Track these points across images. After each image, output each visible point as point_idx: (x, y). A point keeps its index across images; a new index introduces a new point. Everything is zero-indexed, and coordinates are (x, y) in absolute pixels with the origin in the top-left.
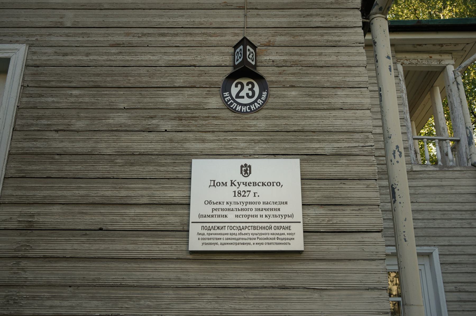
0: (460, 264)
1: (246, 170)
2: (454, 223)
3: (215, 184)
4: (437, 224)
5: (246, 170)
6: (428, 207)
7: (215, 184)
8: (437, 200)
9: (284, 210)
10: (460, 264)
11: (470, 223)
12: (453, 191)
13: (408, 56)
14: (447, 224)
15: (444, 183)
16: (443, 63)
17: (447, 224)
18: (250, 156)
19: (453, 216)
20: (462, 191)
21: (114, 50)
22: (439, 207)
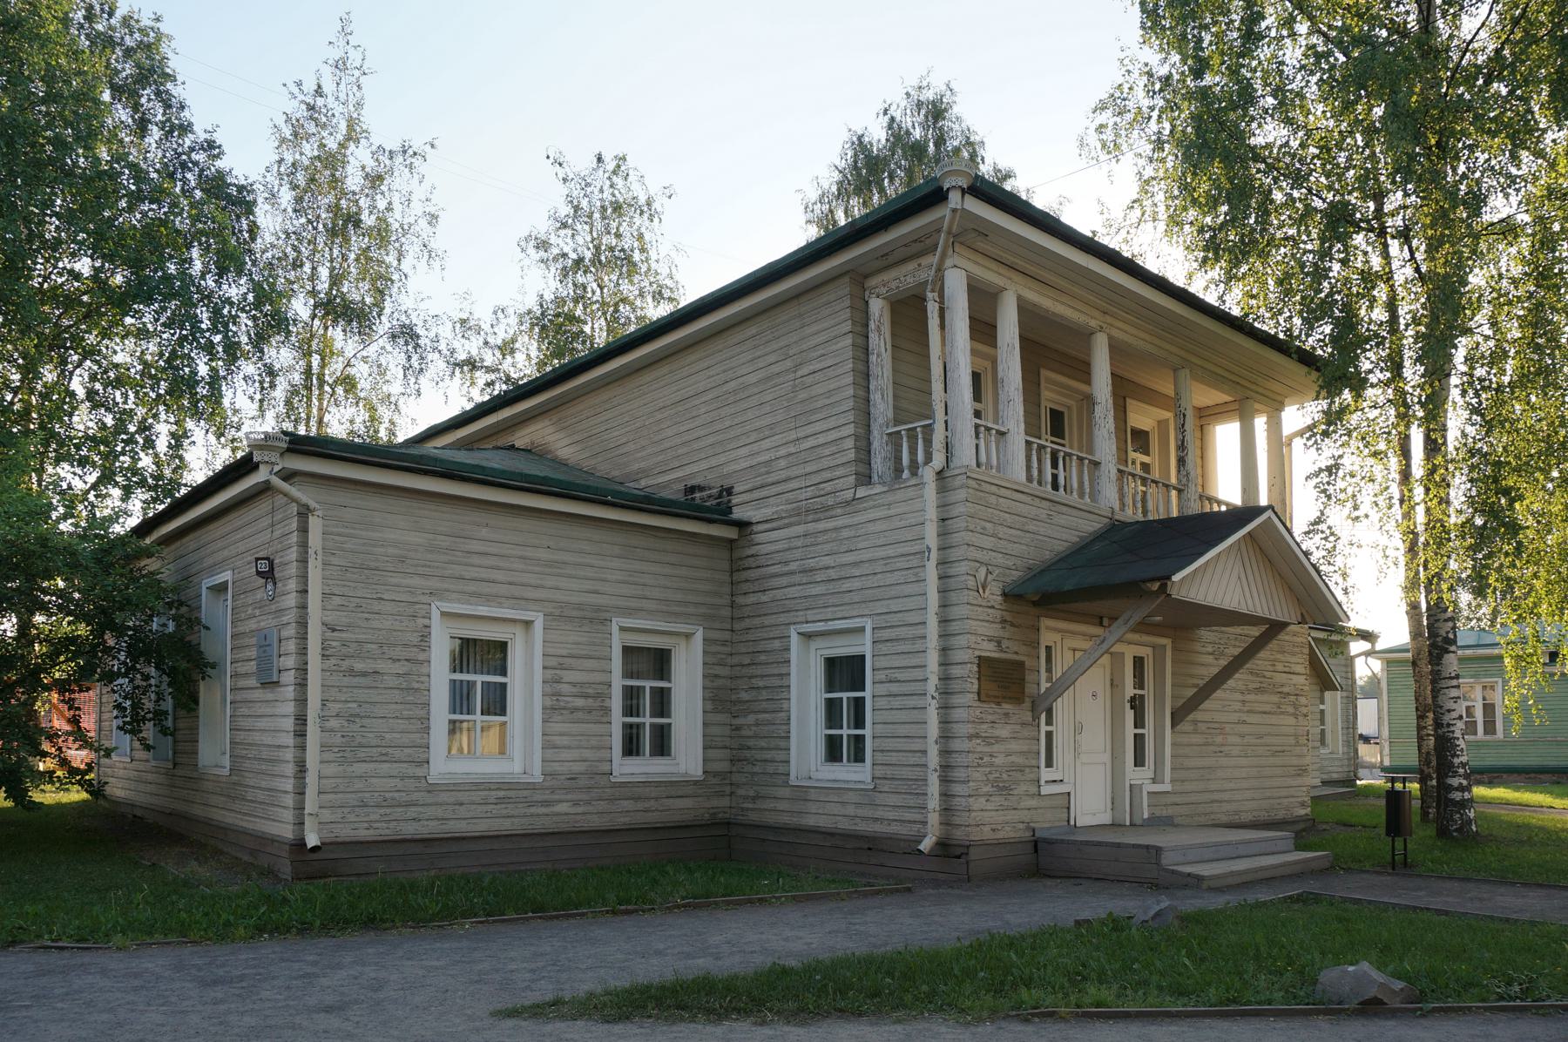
0: (897, 640)
10: (897, 640)
11: (916, 574)
12: (903, 523)
14: (890, 579)
15: (892, 512)
17: (890, 579)
19: (899, 565)
22: (881, 553)
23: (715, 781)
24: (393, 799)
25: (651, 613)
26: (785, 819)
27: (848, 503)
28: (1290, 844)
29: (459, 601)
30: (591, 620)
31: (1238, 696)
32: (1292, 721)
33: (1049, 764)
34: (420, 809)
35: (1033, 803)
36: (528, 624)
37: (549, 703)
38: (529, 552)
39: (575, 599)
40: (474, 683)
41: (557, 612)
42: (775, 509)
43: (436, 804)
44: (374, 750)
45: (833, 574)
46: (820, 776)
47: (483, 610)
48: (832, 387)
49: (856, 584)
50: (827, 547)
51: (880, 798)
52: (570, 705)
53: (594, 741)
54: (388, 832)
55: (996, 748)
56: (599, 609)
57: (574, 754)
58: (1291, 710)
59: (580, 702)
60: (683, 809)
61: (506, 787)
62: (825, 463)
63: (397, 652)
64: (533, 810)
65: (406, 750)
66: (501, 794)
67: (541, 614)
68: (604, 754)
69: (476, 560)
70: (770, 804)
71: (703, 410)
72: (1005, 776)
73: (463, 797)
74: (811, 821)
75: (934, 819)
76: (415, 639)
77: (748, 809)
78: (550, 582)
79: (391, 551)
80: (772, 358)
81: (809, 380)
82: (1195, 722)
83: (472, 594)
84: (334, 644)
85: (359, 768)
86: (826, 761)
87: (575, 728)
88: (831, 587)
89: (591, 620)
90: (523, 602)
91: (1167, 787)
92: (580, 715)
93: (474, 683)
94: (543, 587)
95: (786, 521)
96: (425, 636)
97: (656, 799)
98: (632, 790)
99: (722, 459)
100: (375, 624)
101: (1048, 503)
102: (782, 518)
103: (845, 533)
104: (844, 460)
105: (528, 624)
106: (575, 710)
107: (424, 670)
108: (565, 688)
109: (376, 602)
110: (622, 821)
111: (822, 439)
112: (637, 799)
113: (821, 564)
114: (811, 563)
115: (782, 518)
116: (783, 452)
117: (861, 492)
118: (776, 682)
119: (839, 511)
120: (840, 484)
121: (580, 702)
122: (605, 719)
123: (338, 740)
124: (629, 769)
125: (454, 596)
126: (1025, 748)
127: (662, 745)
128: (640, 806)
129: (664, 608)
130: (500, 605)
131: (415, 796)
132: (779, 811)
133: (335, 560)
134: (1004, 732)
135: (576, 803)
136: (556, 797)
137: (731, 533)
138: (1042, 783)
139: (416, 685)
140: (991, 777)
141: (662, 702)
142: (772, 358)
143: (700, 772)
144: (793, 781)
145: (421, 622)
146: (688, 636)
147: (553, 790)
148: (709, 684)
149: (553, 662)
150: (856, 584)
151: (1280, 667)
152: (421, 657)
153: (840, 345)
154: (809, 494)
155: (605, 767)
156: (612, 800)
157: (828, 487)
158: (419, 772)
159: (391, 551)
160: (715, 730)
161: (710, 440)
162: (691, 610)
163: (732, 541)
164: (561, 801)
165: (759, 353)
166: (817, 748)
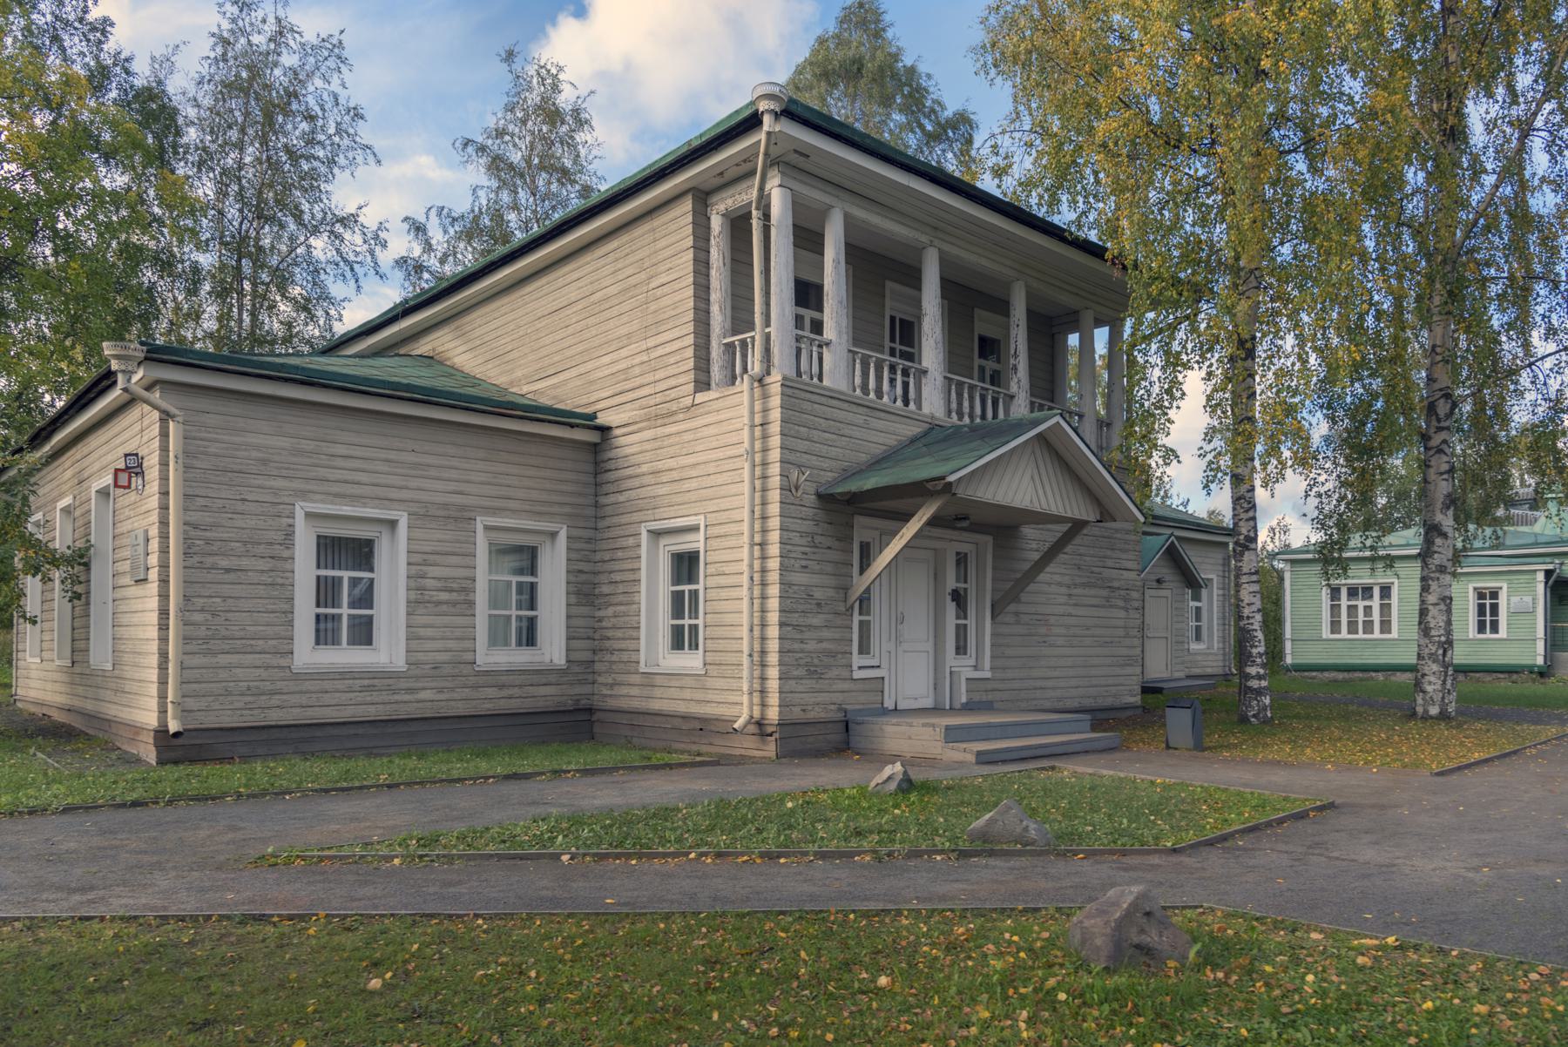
14: (720, 479)
17: (720, 479)
23: (577, 669)
24: (257, 687)
25: (515, 512)
26: (636, 704)
27: (688, 408)
28: (1088, 728)
29: (323, 502)
30: (456, 519)
31: (1064, 590)
32: (1122, 614)
33: (864, 649)
34: (285, 697)
35: (846, 686)
36: (393, 524)
37: (413, 595)
38: (392, 455)
39: (440, 498)
40: (340, 579)
41: (422, 511)
43: (301, 692)
44: (238, 642)
45: (675, 475)
47: (347, 510)
48: (677, 299)
51: (710, 682)
52: (435, 599)
53: (458, 632)
54: (252, 718)
55: (807, 635)
56: (463, 508)
57: (439, 645)
58: (1121, 603)
59: (444, 596)
60: (546, 696)
61: (370, 675)
63: (261, 549)
64: (397, 697)
65: (270, 642)
66: (366, 682)
67: (405, 514)
68: (467, 644)
69: (340, 462)
70: (624, 690)
71: (574, 320)
72: (816, 661)
73: (327, 685)
74: (656, 705)
76: (279, 537)
77: (606, 696)
78: (414, 483)
79: (255, 454)
80: (629, 271)
81: (659, 292)
82: (1017, 614)
83: (336, 495)
84: (198, 542)
85: (224, 659)
86: (673, 648)
87: (439, 620)
89: (456, 519)
90: (386, 502)
91: (988, 675)
92: (444, 608)
93: (340, 579)
94: (407, 488)
96: (289, 534)
97: (520, 686)
98: (493, 677)
99: (589, 366)
100: (239, 523)
101: (865, 410)
103: (687, 437)
104: (685, 368)
105: (393, 524)
106: (439, 603)
107: (288, 566)
108: (429, 583)
109: (240, 503)
110: (486, 707)
111: (668, 348)
112: (502, 687)
113: (666, 466)
114: (660, 465)
116: (637, 360)
117: (700, 397)
118: (630, 576)
121: (444, 596)
122: (469, 612)
123: (202, 632)
124: (489, 657)
125: (318, 497)
126: (837, 636)
127: (529, 636)
128: (506, 692)
129: (528, 508)
130: (365, 505)
131: (279, 685)
132: (629, 697)
133: (197, 464)
134: (816, 621)
135: (440, 690)
136: (420, 685)
137: (592, 437)
138: (855, 667)
139: (280, 581)
140: (802, 662)
141: (530, 596)
142: (629, 271)
143: (563, 662)
144: (643, 668)
145: (286, 521)
146: (553, 535)
147: (417, 678)
148: (573, 579)
149: (417, 558)
150: (693, 484)
151: (1110, 563)
152: (286, 554)
153: (684, 259)
154: (658, 400)
155: (468, 657)
156: (476, 687)
158: (283, 662)
159: (255, 454)
160: (576, 622)
161: (580, 348)
162: (556, 509)
163: (595, 445)
164: (424, 689)
165: (620, 266)
166: (664, 637)
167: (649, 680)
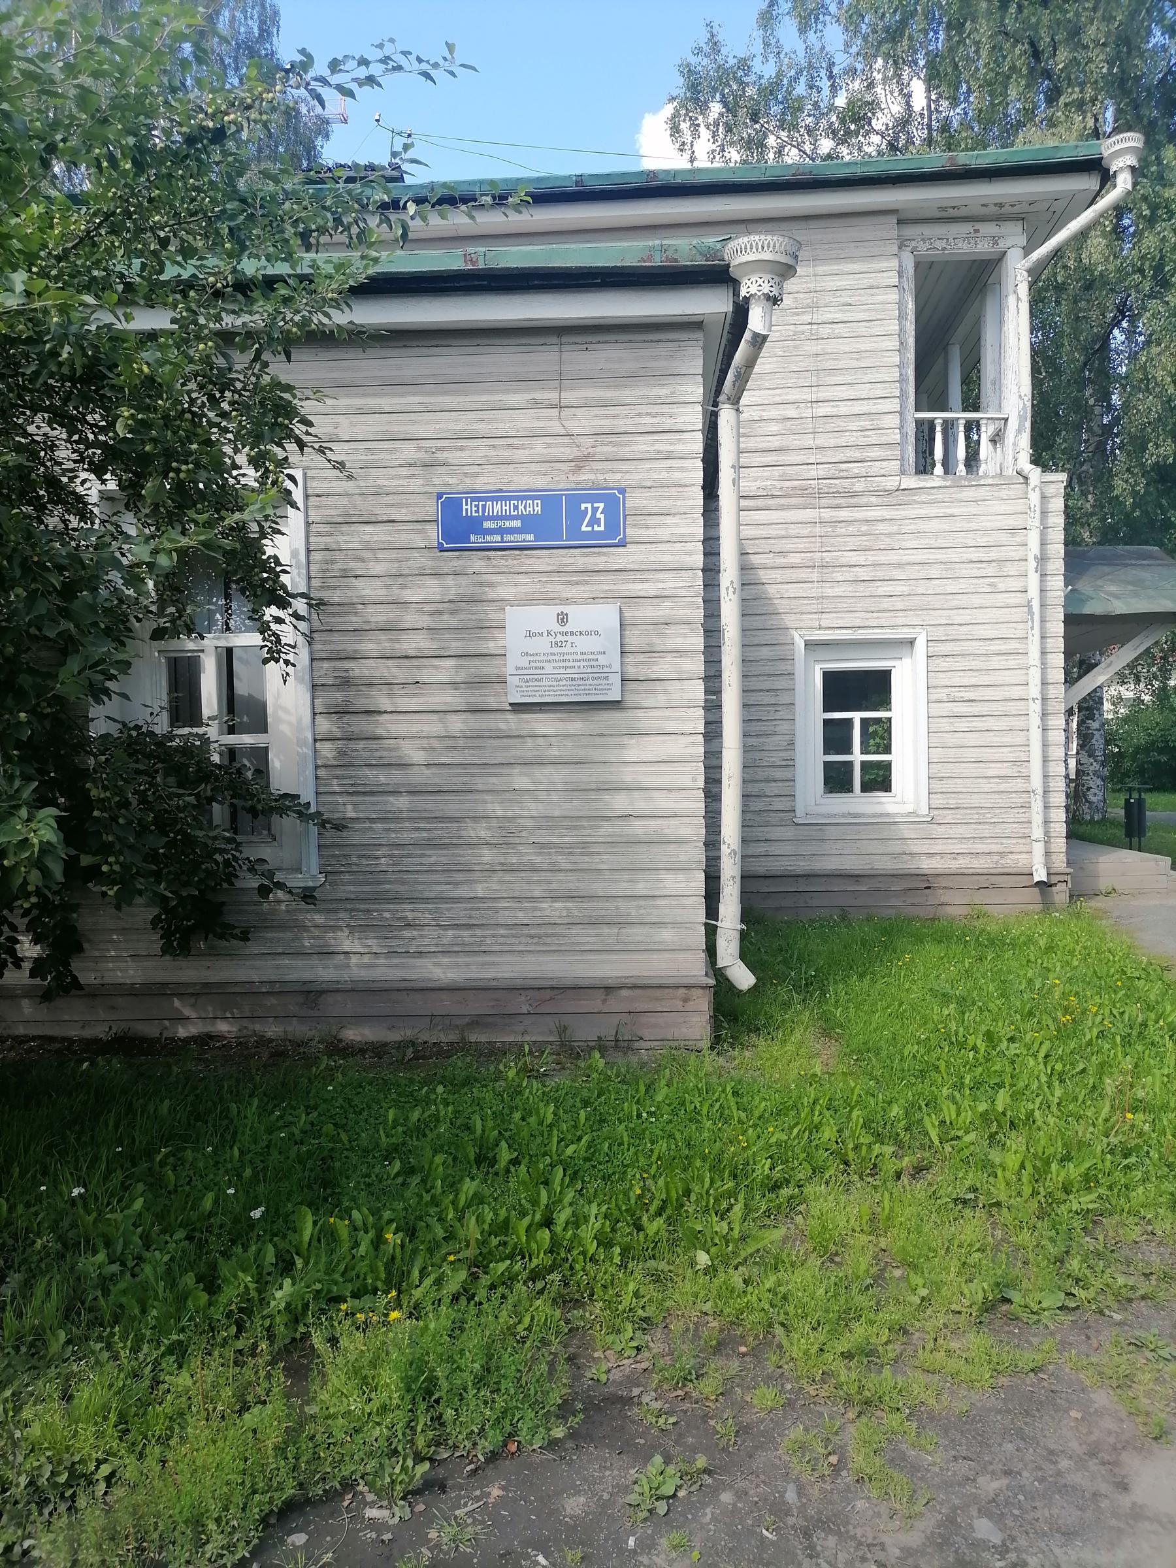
1: (563, 618)
2: (962, 585)
3: (531, 634)
4: (930, 587)
5: (563, 618)
6: (920, 556)
7: (531, 634)
8: (941, 542)
9: (602, 660)
12: (973, 526)
13: (928, 230)
14: (952, 586)
16: (1002, 245)
17: (952, 586)
18: (567, 601)
19: (964, 573)
20: (989, 525)
21: (405, 471)
26: (803, 866)
27: (888, 492)
42: (759, 484)
45: (862, 573)
46: (822, 810)
48: (863, 347)
49: (900, 588)
50: (852, 542)
51: (938, 831)
62: (851, 439)
75: (1038, 849)
88: (861, 589)
95: (782, 501)
102: (773, 496)
103: (882, 528)
104: (884, 440)
111: (843, 409)
113: (843, 561)
115: (773, 496)
116: (774, 413)
119: (873, 500)
120: (876, 467)
150: (900, 588)
153: (878, 298)
154: (821, 473)
157: (855, 469)
167: (817, 831)
